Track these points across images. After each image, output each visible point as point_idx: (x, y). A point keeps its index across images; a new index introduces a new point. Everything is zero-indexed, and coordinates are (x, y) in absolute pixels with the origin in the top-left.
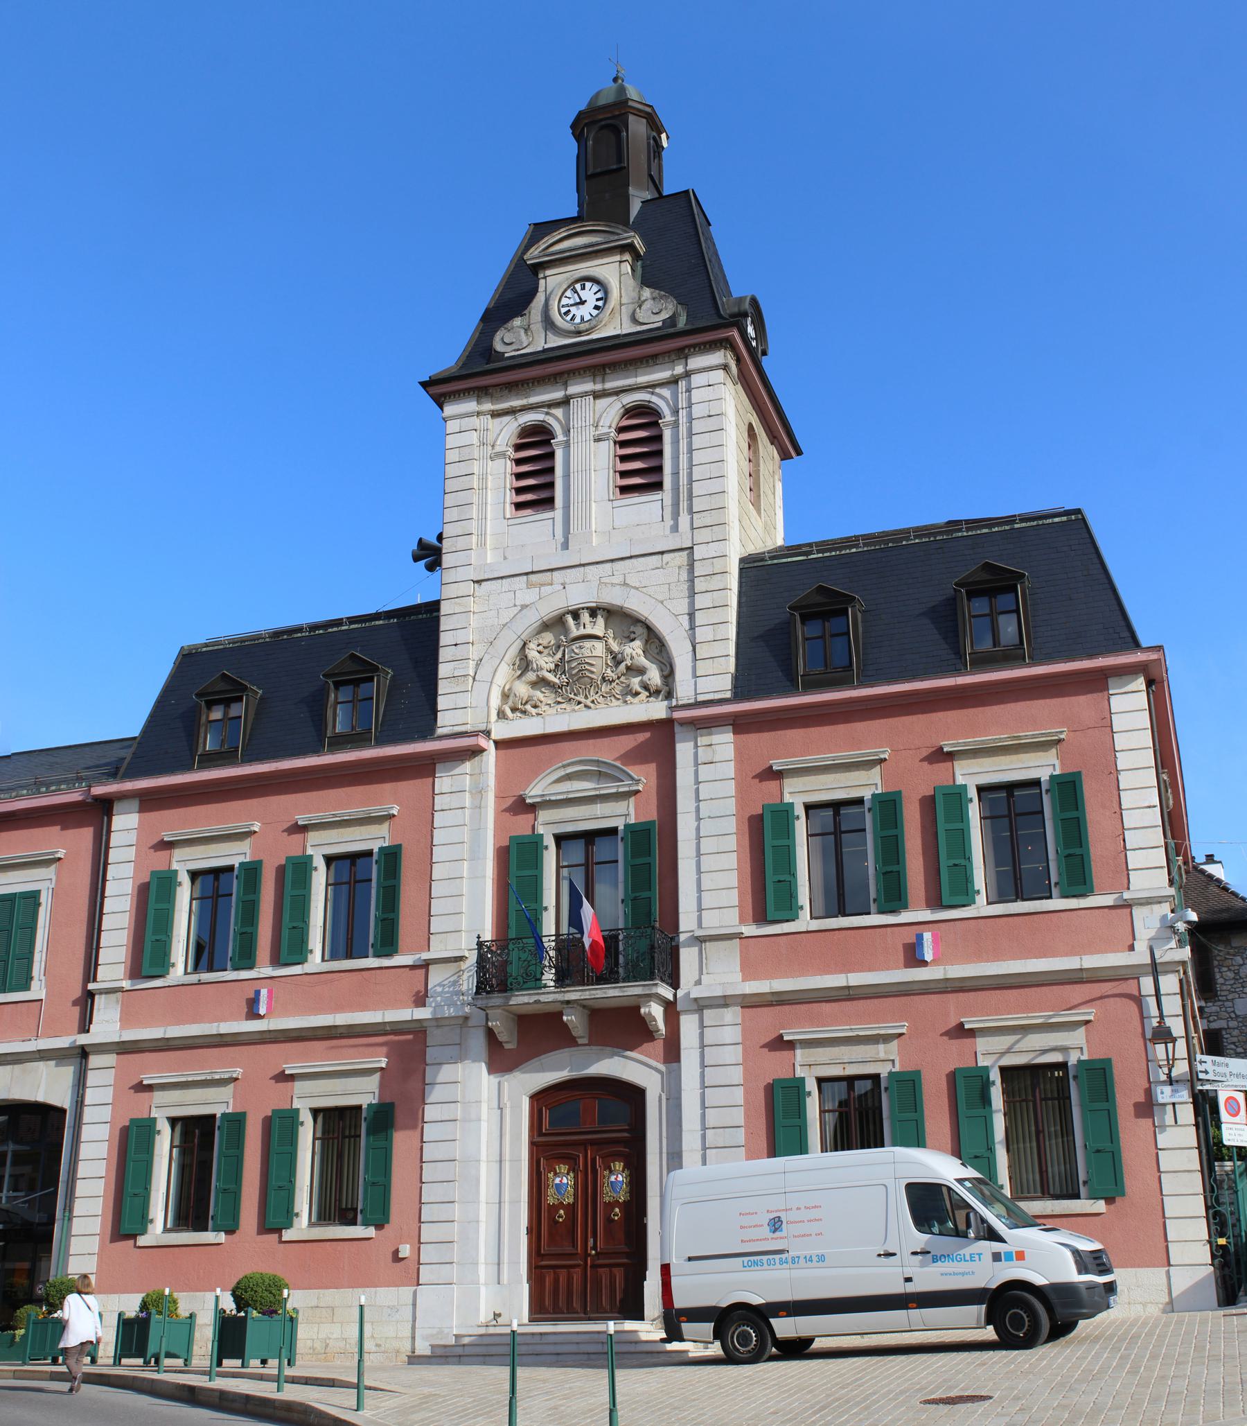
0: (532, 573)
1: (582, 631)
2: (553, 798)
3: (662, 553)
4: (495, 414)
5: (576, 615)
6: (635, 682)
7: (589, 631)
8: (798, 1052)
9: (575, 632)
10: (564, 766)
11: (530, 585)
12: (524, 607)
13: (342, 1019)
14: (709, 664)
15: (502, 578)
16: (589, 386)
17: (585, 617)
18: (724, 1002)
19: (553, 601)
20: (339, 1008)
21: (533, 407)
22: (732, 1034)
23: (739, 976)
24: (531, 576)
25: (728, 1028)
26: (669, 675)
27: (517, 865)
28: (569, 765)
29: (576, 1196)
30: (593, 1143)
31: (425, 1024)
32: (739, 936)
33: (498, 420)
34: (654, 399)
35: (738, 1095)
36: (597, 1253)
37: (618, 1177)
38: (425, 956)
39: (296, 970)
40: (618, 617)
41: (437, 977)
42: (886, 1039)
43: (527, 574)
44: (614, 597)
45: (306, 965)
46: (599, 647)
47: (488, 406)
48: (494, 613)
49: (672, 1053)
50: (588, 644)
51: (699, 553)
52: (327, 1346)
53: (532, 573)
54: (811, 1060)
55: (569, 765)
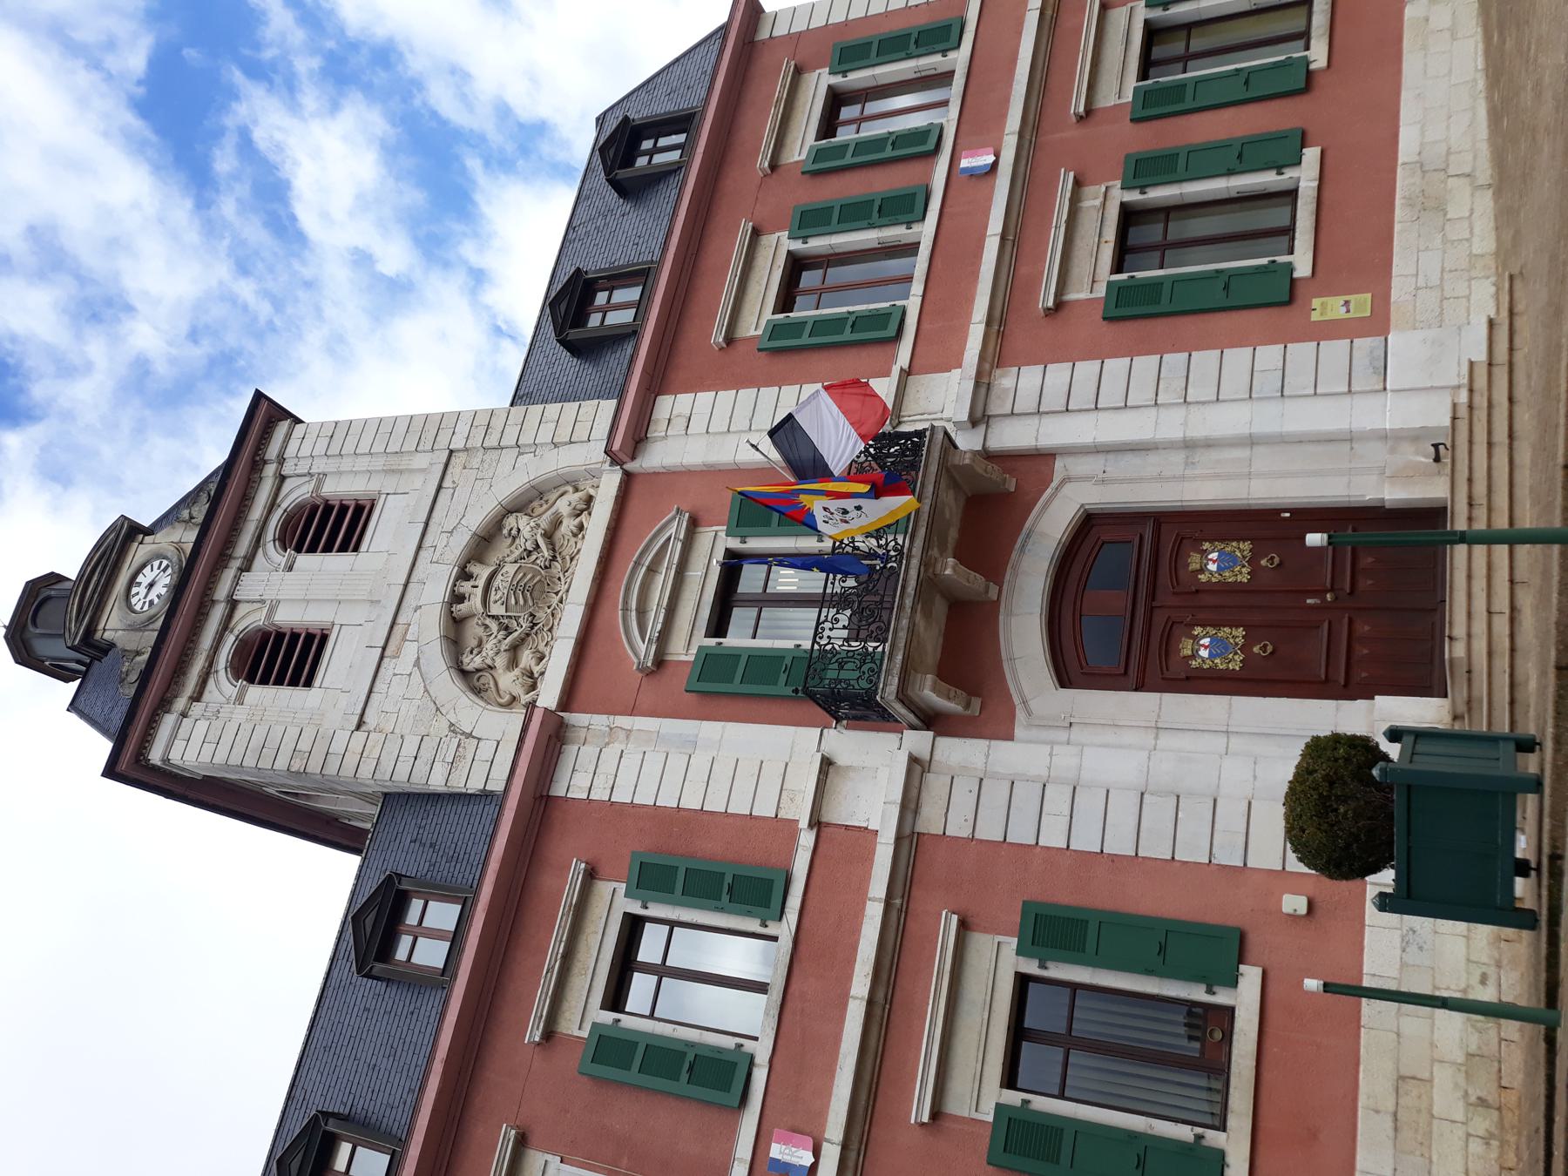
0: (384, 649)
1: (479, 592)
2: (659, 627)
3: (440, 487)
4: (197, 697)
5: (458, 598)
6: (568, 525)
7: (481, 582)
8: (1071, 296)
9: (475, 602)
10: (626, 609)
11: (396, 656)
12: (417, 663)
13: (860, 986)
14: (580, 432)
15: (370, 691)
16: (228, 575)
17: (465, 587)
18: (983, 384)
19: (427, 622)
20: (843, 998)
21: (217, 645)
22: (1030, 377)
23: (956, 372)
24: (388, 653)
25: (1022, 383)
26: (571, 482)
27: (731, 685)
28: (626, 602)
29: (1233, 625)
30: (1152, 595)
31: (907, 831)
32: (906, 374)
33: (206, 696)
34: (284, 505)
35: (1116, 366)
36: (1332, 590)
37: (1213, 563)
38: (804, 823)
39: (760, 1076)
40: (483, 543)
41: (843, 811)
42: (1075, 200)
43: (382, 657)
44: (460, 543)
45: (757, 1060)
46: (510, 569)
47: (180, 704)
48: (405, 705)
49: (1038, 462)
50: (497, 582)
51: (458, 443)
52: (1482, 1102)
53: (384, 649)
54: (1087, 281)
55: (626, 602)
